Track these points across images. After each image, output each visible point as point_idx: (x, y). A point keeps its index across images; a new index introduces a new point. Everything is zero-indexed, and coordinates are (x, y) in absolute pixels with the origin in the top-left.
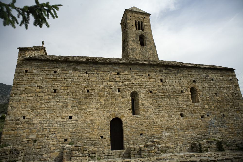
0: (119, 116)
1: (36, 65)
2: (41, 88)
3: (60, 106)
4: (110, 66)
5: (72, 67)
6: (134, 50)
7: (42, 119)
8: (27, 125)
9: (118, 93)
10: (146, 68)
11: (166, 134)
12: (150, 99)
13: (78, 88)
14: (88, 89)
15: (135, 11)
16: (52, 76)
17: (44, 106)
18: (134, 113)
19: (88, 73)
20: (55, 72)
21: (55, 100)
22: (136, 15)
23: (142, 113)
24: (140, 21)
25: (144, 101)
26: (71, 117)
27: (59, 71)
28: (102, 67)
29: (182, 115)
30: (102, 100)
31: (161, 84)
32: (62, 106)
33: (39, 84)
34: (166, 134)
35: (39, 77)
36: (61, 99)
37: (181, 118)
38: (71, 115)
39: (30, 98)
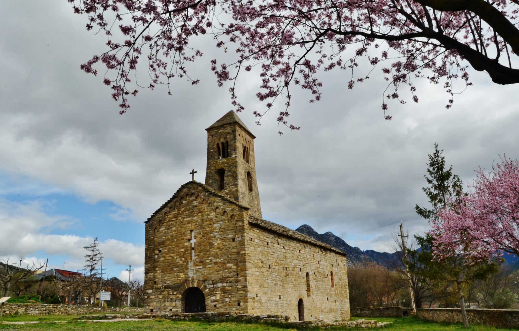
0: (302, 298)
1: (256, 233)
2: (262, 262)
3: (273, 284)
4: (295, 242)
5: (277, 239)
6: (243, 194)
7: (266, 298)
8: (259, 304)
9: (300, 273)
10: (313, 249)
11: (322, 316)
12: (314, 281)
13: (281, 265)
14: (287, 266)
15: (244, 128)
16: (266, 248)
17: (266, 284)
18: (309, 295)
19: (285, 247)
20: (267, 243)
21: (270, 277)
22: (243, 133)
23: (311, 295)
24: (247, 146)
25: (312, 283)
26: (280, 298)
27: (270, 244)
28: (293, 244)
29: (328, 299)
30: (293, 279)
31: (318, 266)
32: (275, 285)
33: (260, 257)
34: (322, 316)
35: (260, 249)
36: (274, 276)
37: (327, 302)
38: (280, 294)
39: (258, 273)
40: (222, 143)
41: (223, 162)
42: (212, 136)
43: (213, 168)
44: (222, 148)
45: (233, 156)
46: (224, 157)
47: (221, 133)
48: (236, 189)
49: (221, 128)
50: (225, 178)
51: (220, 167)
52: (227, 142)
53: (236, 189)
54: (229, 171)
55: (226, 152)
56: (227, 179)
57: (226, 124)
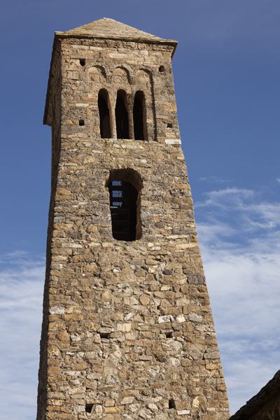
40: (121, 93)
41: (131, 150)
42: (83, 62)
43: (91, 160)
44: (116, 110)
45: (169, 142)
46: (123, 134)
47: (114, 60)
48: (191, 245)
49: (116, 46)
50: (144, 203)
51: (121, 163)
52: (140, 96)
53: (191, 245)
54: (161, 184)
55: (132, 124)
56: (149, 209)
57: (137, 41)
